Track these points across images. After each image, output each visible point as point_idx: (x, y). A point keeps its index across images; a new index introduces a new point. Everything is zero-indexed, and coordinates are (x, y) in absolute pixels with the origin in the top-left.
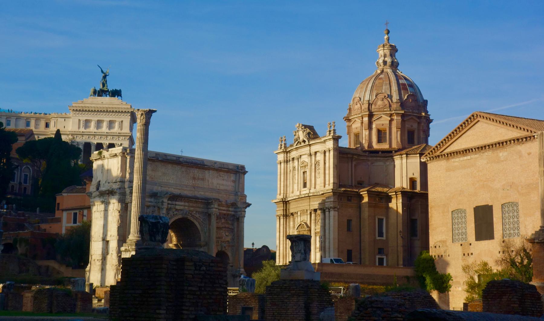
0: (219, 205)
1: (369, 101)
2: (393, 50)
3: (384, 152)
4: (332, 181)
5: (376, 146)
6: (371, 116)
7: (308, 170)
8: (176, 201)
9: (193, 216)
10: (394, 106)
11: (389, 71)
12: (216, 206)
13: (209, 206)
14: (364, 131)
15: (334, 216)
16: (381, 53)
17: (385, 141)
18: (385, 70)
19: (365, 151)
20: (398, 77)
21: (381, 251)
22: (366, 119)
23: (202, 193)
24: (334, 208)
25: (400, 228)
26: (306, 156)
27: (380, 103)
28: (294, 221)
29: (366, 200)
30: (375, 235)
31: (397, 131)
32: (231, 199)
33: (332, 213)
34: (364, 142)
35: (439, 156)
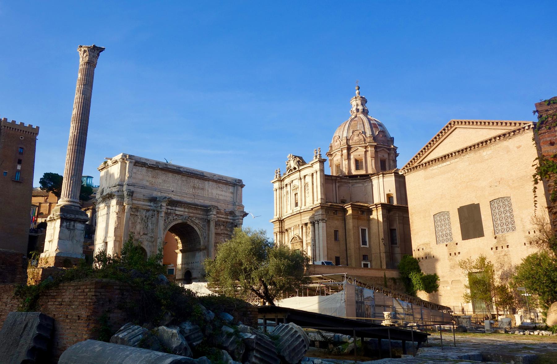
0: (218, 213)
1: (347, 137)
2: (364, 101)
3: (361, 176)
4: (319, 197)
5: (354, 172)
6: (349, 148)
7: (298, 191)
8: (176, 207)
9: (192, 221)
10: (368, 140)
11: (362, 116)
12: (215, 213)
13: (209, 214)
14: (344, 161)
15: (323, 227)
16: (354, 103)
17: (362, 169)
18: (358, 116)
19: (346, 176)
20: (369, 120)
21: (365, 257)
22: (345, 152)
23: (202, 201)
24: (323, 220)
25: (382, 236)
26: (297, 180)
27: (356, 138)
28: (288, 236)
29: (350, 212)
30: (359, 243)
32: (230, 208)
33: (321, 224)
34: (344, 170)
35: (416, 167)
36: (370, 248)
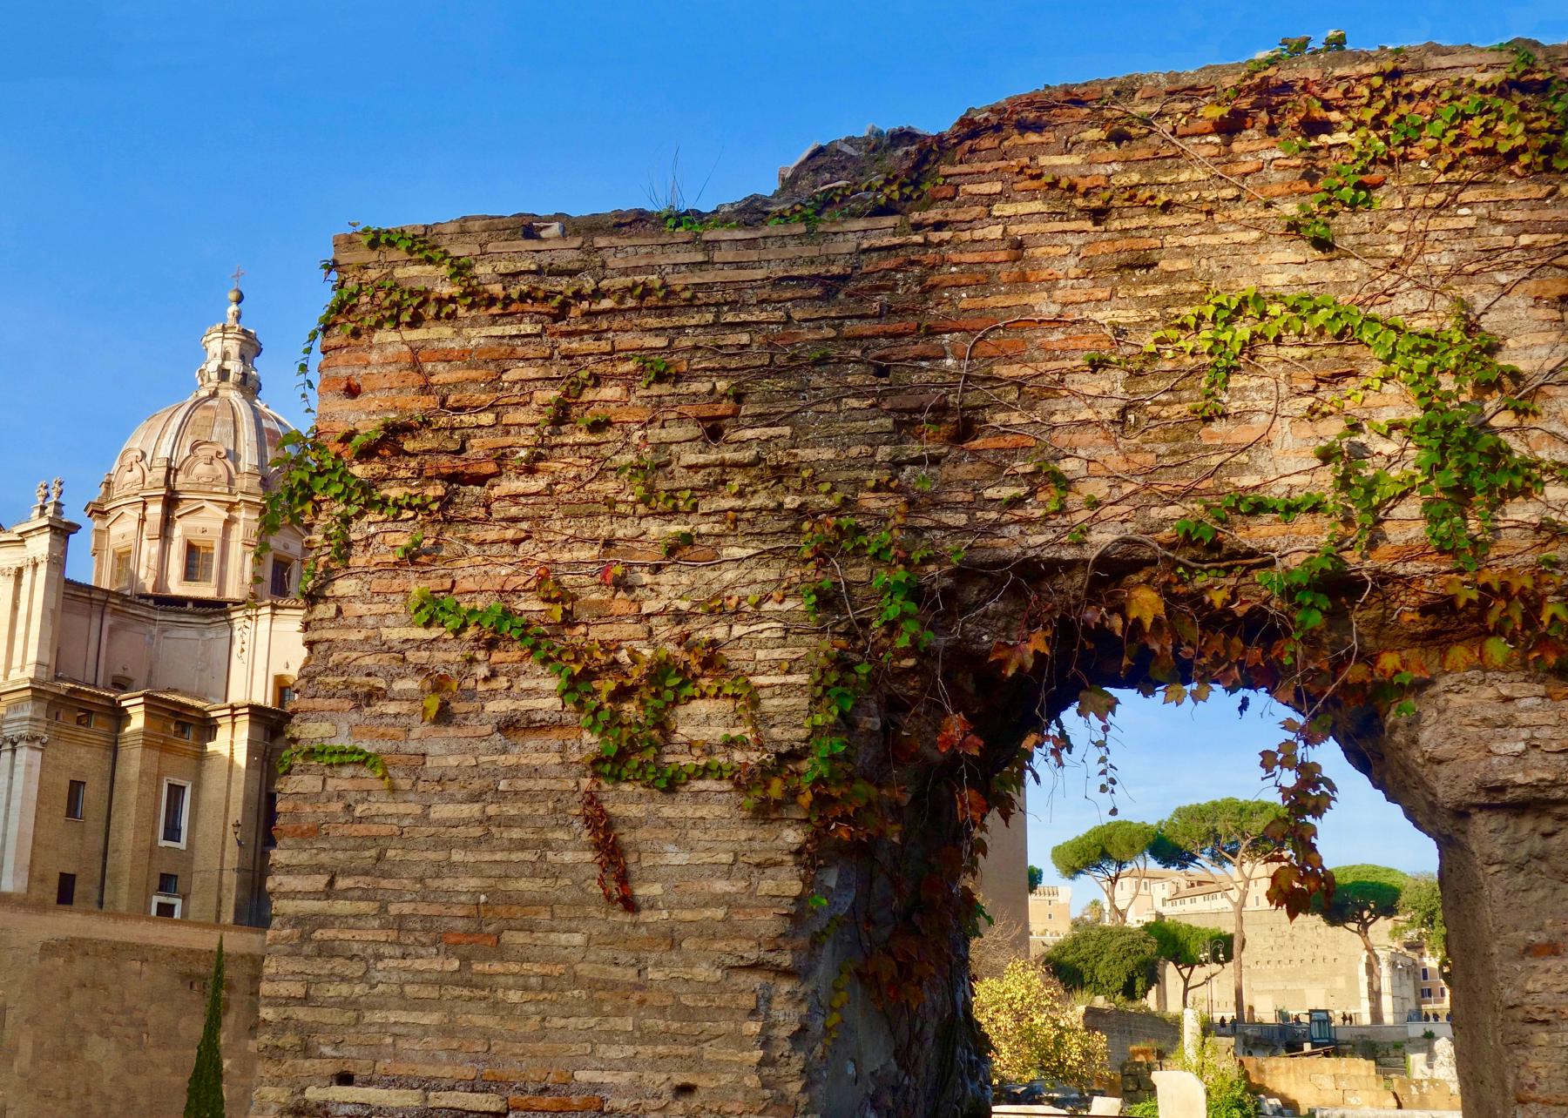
1: (169, 460)
2: (251, 347)
3: (199, 603)
4: (33, 656)
5: (176, 586)
6: (171, 501)
10: (242, 483)
11: (235, 396)
14: (145, 543)
15: (29, 765)
16: (215, 346)
17: (207, 578)
18: (221, 393)
19: (147, 597)
20: (258, 416)
21: (167, 883)
22: (155, 510)
25: (236, 813)
27: (201, 469)
29: (137, 721)
30: (154, 832)
31: (245, 553)
33: (23, 753)
34: (142, 574)
36: (188, 856)
